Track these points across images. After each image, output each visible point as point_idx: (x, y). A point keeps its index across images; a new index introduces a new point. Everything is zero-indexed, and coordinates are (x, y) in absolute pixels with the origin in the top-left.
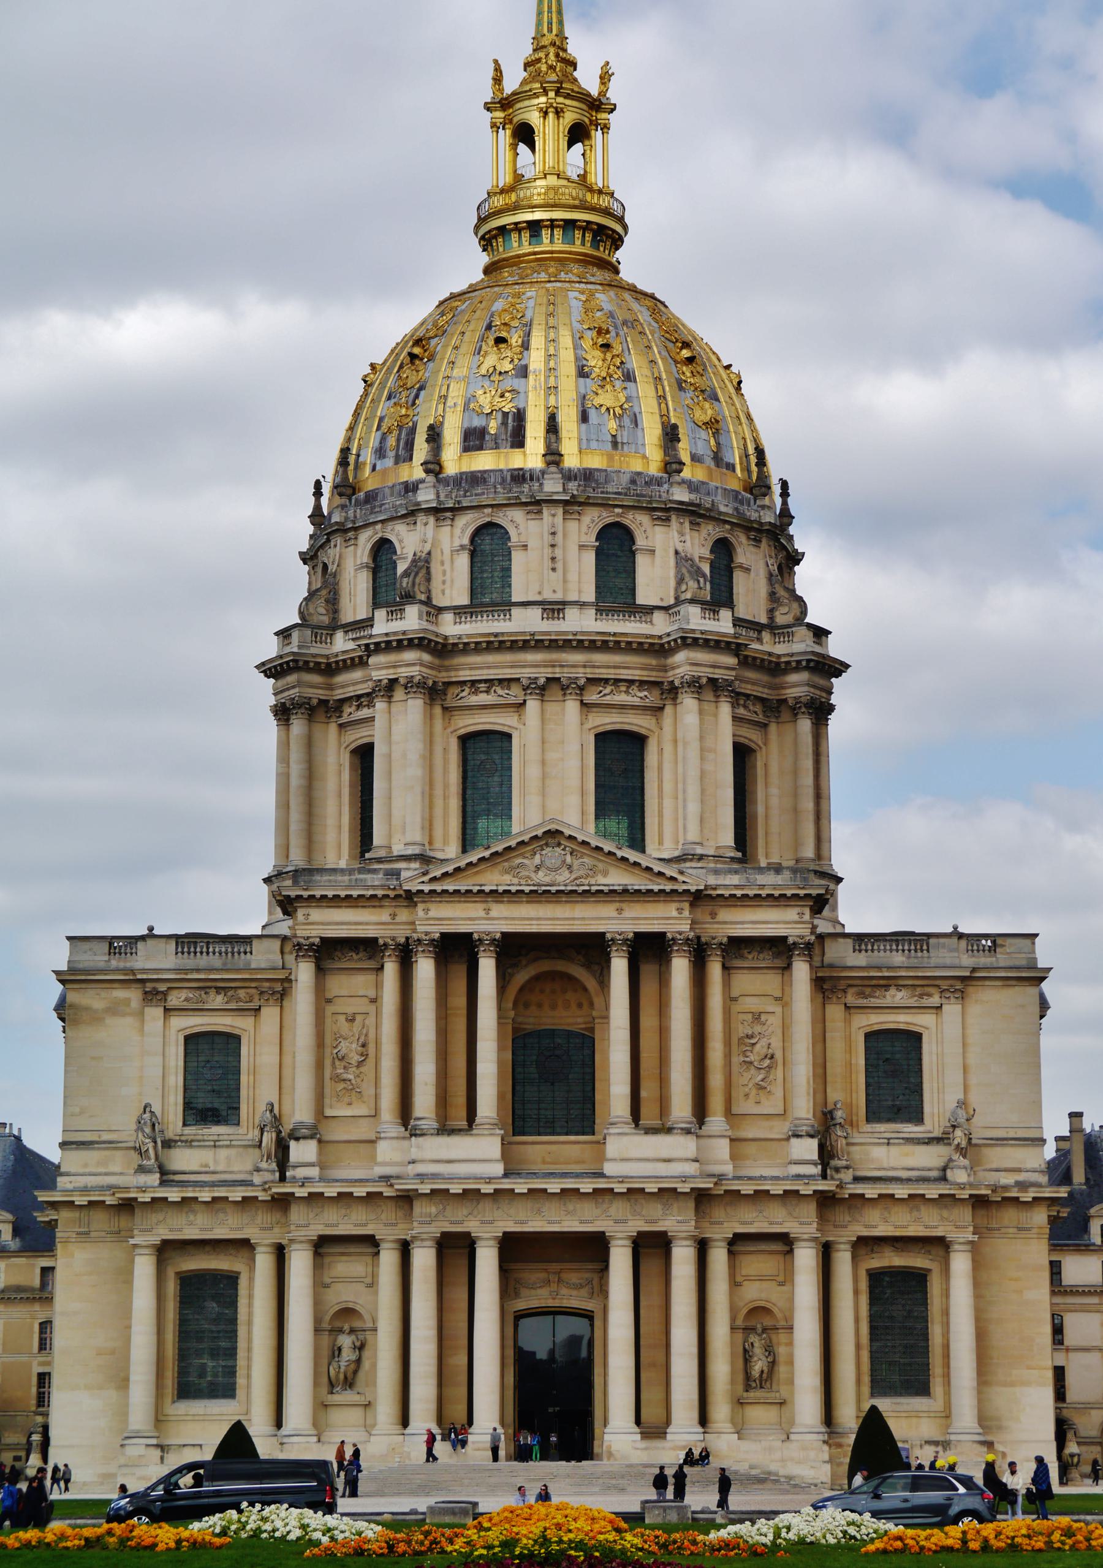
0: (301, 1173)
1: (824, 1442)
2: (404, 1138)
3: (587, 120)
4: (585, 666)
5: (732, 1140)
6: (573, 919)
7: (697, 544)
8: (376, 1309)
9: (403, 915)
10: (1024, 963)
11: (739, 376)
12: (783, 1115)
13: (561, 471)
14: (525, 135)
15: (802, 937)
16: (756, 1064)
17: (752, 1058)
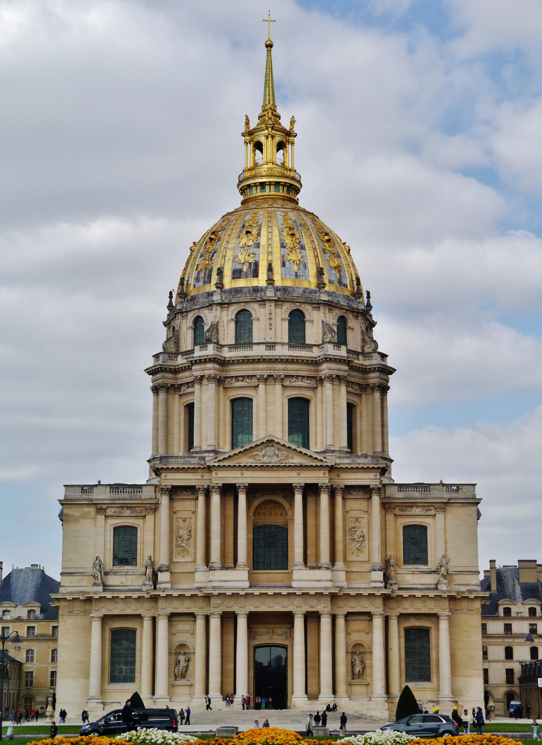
0: (163, 586)
1: (386, 701)
2: (207, 571)
3: (285, 140)
4: (284, 370)
5: (346, 572)
6: (279, 478)
7: (332, 318)
8: (195, 645)
9: (207, 476)
10: (470, 496)
11: (349, 247)
13: (274, 287)
14: (259, 146)
15: (376, 485)
17: (355, 537)
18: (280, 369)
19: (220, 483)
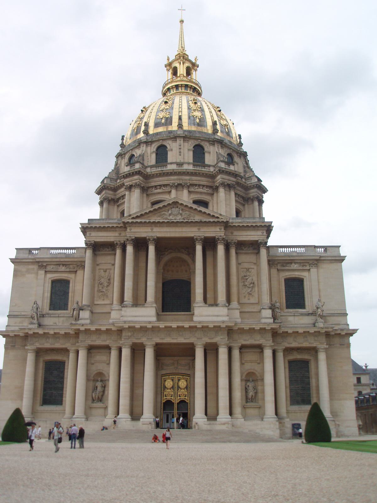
2: (121, 310)
4: (189, 180)
5: (240, 312)
6: (182, 232)
7: (223, 152)
8: (109, 372)
9: (123, 234)
12: (258, 304)
16: (248, 286)
17: (246, 283)
18: (186, 179)
19: (133, 236)
